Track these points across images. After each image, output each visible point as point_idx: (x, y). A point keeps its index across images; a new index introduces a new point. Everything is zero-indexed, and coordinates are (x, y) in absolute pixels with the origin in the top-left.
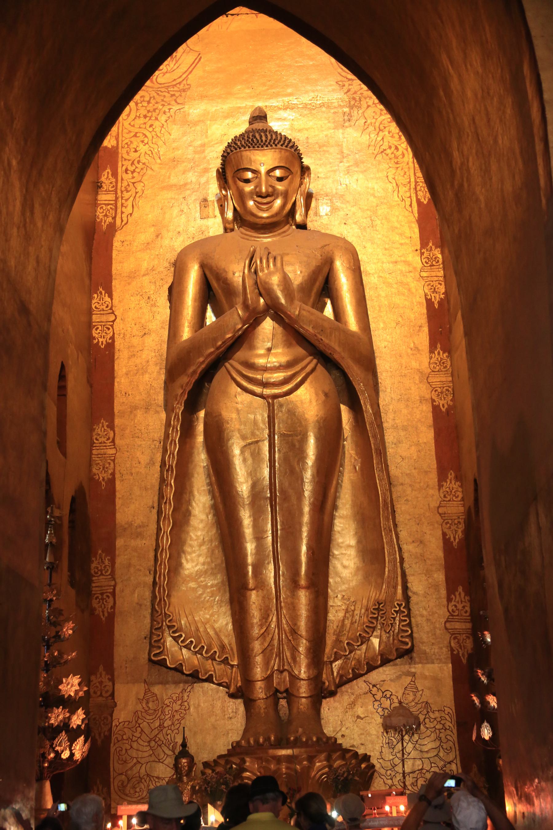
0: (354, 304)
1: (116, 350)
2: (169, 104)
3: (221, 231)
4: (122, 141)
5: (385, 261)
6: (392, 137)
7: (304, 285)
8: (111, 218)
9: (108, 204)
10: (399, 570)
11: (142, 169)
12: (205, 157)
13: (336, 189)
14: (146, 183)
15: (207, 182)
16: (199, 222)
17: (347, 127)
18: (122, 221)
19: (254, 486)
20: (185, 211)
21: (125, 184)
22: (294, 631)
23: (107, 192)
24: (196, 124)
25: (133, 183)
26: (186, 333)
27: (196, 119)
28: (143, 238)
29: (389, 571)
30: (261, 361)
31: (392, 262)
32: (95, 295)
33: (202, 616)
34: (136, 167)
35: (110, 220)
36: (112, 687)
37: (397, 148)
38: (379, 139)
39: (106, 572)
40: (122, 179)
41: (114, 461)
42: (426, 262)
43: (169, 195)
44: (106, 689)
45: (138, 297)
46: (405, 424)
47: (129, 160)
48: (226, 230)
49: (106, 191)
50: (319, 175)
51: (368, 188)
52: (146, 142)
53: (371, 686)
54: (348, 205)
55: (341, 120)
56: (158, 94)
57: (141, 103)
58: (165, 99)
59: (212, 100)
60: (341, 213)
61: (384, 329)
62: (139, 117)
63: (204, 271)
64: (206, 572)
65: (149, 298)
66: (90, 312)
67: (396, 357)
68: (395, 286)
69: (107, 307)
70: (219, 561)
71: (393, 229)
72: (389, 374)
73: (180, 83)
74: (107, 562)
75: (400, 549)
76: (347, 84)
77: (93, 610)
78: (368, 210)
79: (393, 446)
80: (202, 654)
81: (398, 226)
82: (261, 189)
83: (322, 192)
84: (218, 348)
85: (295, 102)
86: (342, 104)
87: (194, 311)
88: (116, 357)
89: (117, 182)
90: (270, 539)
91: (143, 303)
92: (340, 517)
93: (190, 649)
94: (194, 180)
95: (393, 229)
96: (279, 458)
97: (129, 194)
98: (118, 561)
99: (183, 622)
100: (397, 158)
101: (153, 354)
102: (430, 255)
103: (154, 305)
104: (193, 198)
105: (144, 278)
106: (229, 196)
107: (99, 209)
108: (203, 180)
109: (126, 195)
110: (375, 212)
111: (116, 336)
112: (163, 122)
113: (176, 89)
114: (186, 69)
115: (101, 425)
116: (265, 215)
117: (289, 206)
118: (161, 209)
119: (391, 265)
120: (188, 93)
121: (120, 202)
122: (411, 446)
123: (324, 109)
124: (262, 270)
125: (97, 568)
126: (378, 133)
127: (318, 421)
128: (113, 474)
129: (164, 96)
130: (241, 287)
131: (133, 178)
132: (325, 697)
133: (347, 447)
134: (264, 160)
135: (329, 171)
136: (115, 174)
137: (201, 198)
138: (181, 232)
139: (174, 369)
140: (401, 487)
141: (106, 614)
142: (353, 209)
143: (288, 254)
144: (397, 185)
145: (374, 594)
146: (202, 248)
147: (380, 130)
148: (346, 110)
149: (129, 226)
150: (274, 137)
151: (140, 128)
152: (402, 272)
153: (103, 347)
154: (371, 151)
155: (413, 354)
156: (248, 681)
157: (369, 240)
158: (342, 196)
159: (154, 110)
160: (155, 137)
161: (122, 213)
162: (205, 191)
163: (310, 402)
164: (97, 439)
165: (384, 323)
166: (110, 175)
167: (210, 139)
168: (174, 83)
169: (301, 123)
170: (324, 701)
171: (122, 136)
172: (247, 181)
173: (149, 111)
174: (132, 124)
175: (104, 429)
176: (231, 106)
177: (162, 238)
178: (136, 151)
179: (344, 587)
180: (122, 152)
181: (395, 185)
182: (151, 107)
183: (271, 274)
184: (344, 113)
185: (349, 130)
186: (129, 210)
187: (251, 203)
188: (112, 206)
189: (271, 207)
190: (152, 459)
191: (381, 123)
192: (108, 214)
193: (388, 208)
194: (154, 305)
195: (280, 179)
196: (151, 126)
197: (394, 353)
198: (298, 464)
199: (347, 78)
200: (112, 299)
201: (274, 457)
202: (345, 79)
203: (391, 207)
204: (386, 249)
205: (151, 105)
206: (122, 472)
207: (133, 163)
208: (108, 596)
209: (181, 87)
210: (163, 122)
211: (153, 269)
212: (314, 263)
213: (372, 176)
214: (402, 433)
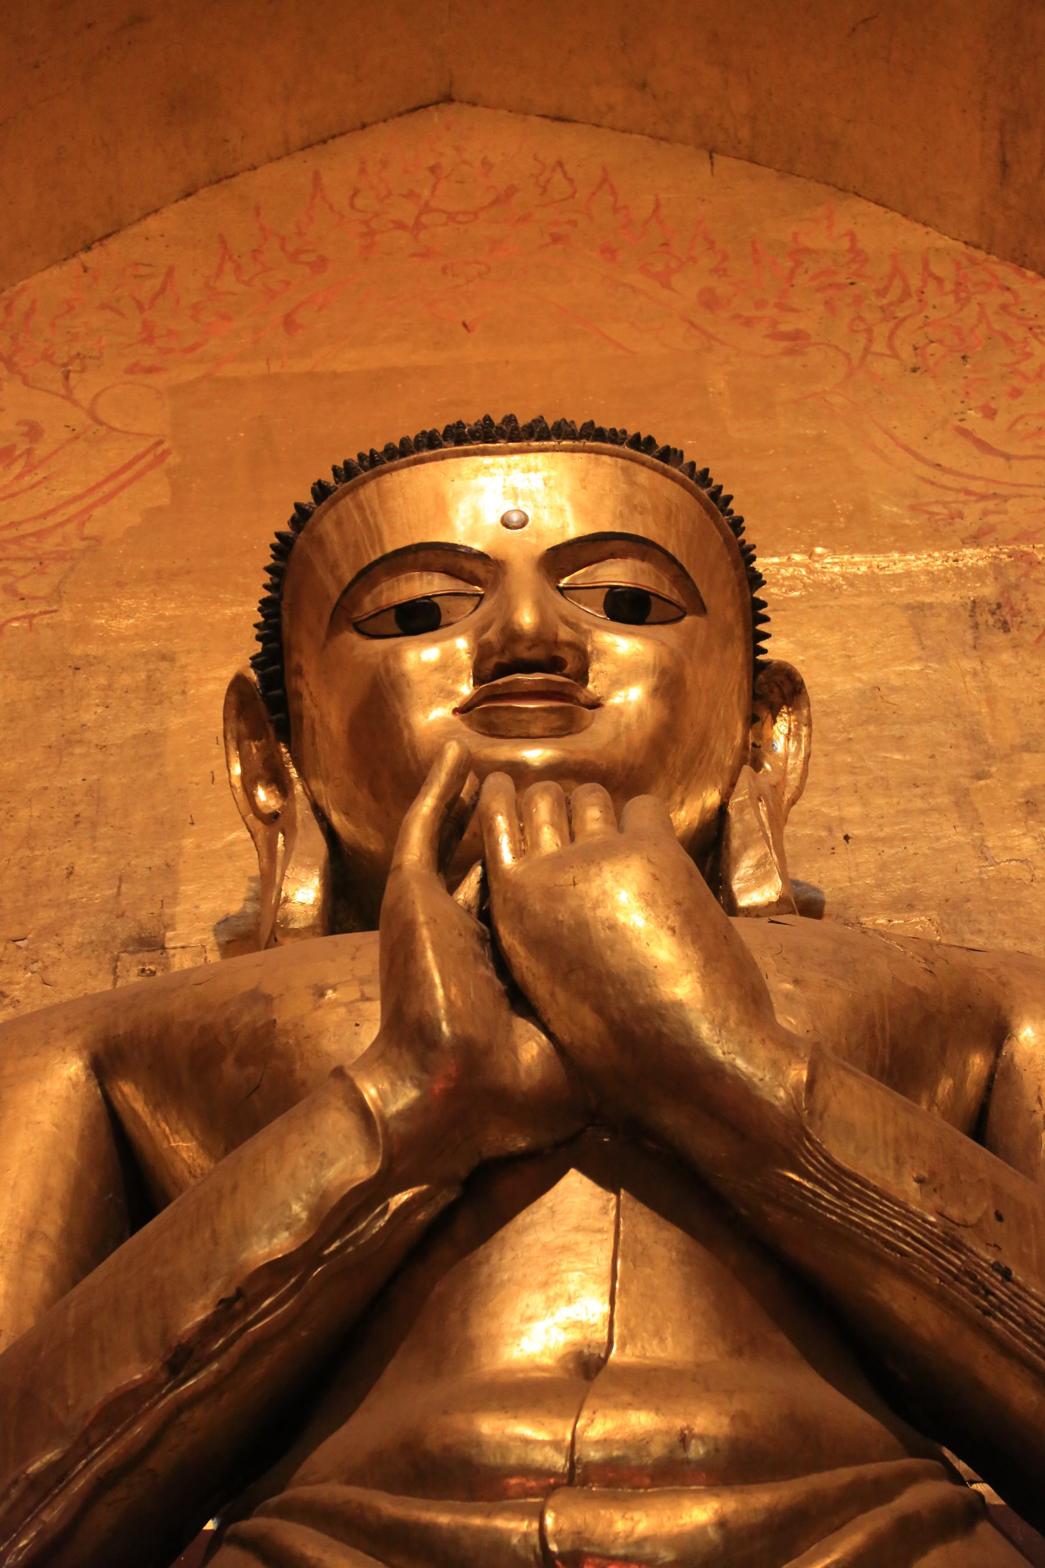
30: (529, 1435)
50: (854, 831)
63: (107, 1100)
73: (39, 535)
84: (181, 1360)
104: (75, 935)
114: (78, 490)
137: (124, 930)
172: (421, 619)
199: (968, 493)
202: (962, 497)
209: (49, 544)
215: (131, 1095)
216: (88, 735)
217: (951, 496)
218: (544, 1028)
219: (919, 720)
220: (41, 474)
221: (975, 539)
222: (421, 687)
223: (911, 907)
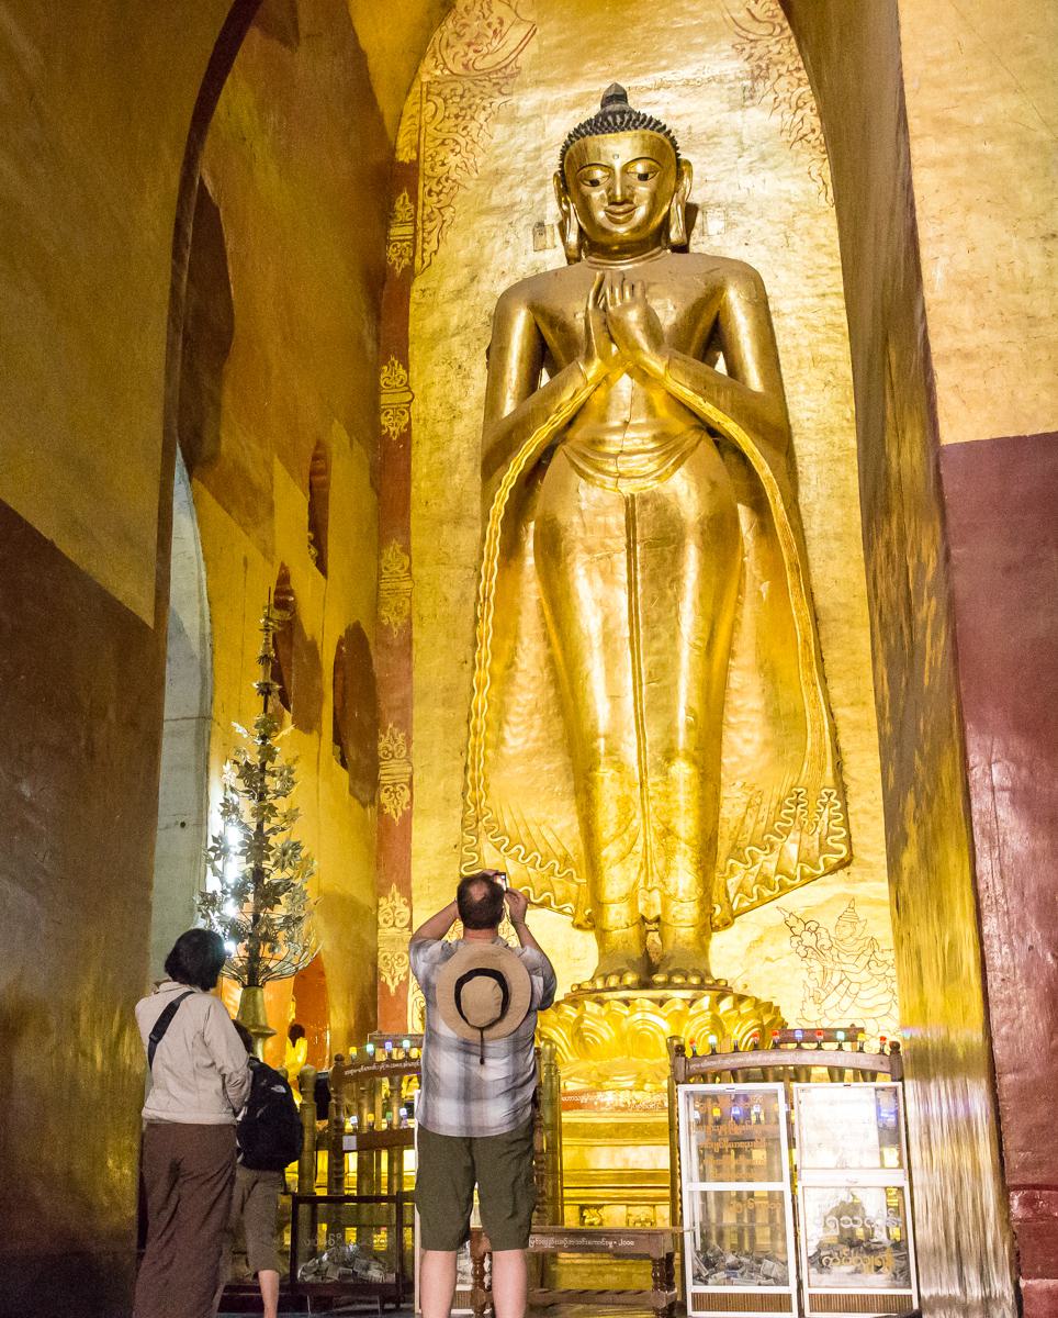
0: (756, 352)
1: (414, 442)
2: (490, 97)
3: (566, 264)
7: (679, 326)
8: (407, 260)
9: (404, 241)
10: (828, 743)
12: (540, 166)
13: (733, 196)
14: (457, 207)
15: (544, 200)
16: (532, 255)
17: (747, 107)
18: (423, 262)
19: (606, 620)
20: (512, 241)
21: (428, 210)
22: (668, 832)
23: (404, 223)
24: (528, 120)
25: (439, 209)
26: (509, 406)
27: (530, 113)
28: (451, 284)
29: (813, 744)
31: (817, 296)
32: (385, 368)
33: (533, 813)
34: (444, 187)
35: (406, 261)
36: (409, 915)
38: (797, 119)
39: (399, 755)
40: (424, 205)
41: (410, 598)
43: (488, 221)
44: (401, 917)
45: (444, 367)
46: (839, 530)
48: (570, 260)
49: (401, 222)
51: (780, 191)
52: (457, 150)
53: (787, 915)
56: (475, 85)
60: (741, 230)
61: (806, 392)
62: (448, 118)
64: (538, 752)
65: (460, 367)
66: (376, 391)
68: (822, 330)
69: (401, 382)
70: (560, 736)
71: (819, 247)
72: (814, 458)
73: (506, 67)
74: (400, 740)
75: (831, 715)
76: (747, 47)
77: (381, 807)
78: (780, 222)
79: (821, 563)
80: (534, 868)
81: (827, 243)
83: (712, 202)
85: (672, 78)
86: (741, 76)
87: (520, 375)
88: (413, 452)
89: (416, 208)
90: (630, 698)
91: (451, 376)
92: (738, 669)
93: (517, 860)
94: (525, 197)
95: (819, 247)
96: (643, 580)
97: (434, 223)
98: (416, 736)
99: (506, 823)
101: (466, 446)
103: (467, 377)
104: (524, 222)
105: (453, 339)
106: (572, 212)
109: (429, 226)
110: (791, 225)
112: (482, 121)
113: (500, 75)
115: (392, 548)
116: (622, 230)
117: (658, 220)
118: (478, 242)
119: (816, 300)
120: (518, 79)
122: (848, 563)
123: (714, 84)
124: (614, 303)
125: (387, 749)
127: (701, 522)
128: (409, 618)
130: (583, 334)
131: (439, 201)
132: (717, 929)
133: (748, 567)
134: (621, 149)
136: (414, 198)
137: (535, 221)
138: (506, 272)
139: (493, 459)
140: (833, 623)
141: (400, 814)
142: (759, 223)
143: (655, 284)
145: (791, 779)
146: (533, 291)
147: (798, 108)
148: (748, 83)
149: (432, 268)
150: (634, 117)
152: (832, 308)
153: (395, 439)
154: (784, 139)
156: (598, 904)
157: (784, 265)
158: (742, 205)
159: (470, 107)
160: (470, 142)
161: (424, 250)
162: (540, 213)
163: (689, 492)
164: (386, 568)
165: (806, 383)
166: (407, 200)
167: (547, 139)
168: (498, 67)
169: (680, 107)
170: (714, 934)
172: (595, 183)
173: (462, 109)
174: (438, 128)
175: (397, 554)
176: (577, 91)
177: (478, 282)
178: (443, 164)
179: (745, 770)
180: (425, 166)
183: (626, 307)
185: (752, 111)
187: (600, 215)
189: (630, 218)
190: (462, 595)
191: (799, 98)
193: (812, 218)
194: (467, 377)
195: (643, 177)
196: (465, 128)
198: (671, 587)
200: (408, 372)
201: (636, 578)
203: (815, 216)
204: (808, 277)
206: (421, 612)
207: (439, 182)
208: (402, 788)
209: (508, 71)
211: (466, 327)
212: (696, 295)
213: (787, 173)
214: (835, 545)
215: (540, 321)
220: (504, 40)
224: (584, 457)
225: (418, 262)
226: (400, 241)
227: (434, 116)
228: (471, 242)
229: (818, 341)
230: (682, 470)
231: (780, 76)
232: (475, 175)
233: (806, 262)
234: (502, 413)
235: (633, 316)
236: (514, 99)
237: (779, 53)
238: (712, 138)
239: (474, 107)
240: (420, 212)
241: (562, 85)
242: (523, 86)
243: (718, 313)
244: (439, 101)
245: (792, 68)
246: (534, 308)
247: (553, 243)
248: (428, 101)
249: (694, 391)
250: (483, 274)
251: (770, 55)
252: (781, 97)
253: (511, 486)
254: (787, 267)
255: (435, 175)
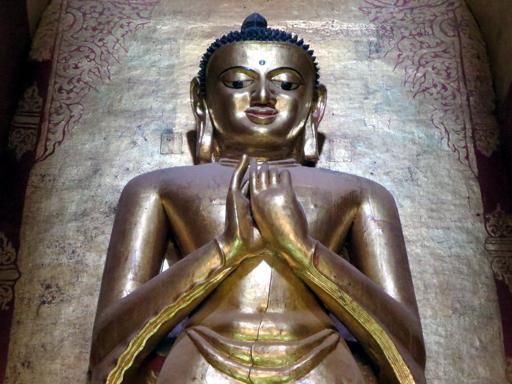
2: (129, 18)
3: (191, 164)
4: (59, 55)
5: (431, 225)
6: (438, 73)
11: (82, 89)
12: (173, 81)
16: (157, 157)
20: (139, 143)
23: (31, 114)
24: (163, 43)
25: (68, 105)
26: (128, 287)
31: (442, 228)
34: (75, 87)
35: (29, 147)
37: (444, 88)
38: (419, 75)
42: (493, 231)
47: (65, 77)
50: (335, 112)
54: (376, 150)
55: (366, 50)
57: (90, 14)
58: (124, 12)
59: (189, 17)
62: (86, 29)
65: (73, 252)
67: (453, 359)
68: (448, 259)
69: (9, 260)
78: (404, 159)
82: (259, 92)
83: (339, 133)
85: (303, 26)
89: (45, 102)
94: (155, 105)
97: (61, 117)
100: (446, 99)
102: (498, 223)
106: (208, 116)
107: (14, 133)
108: (169, 107)
111: (16, 300)
112: (119, 36)
116: (262, 130)
117: (294, 132)
119: (441, 231)
120: (156, 7)
121: (46, 126)
123: (341, 36)
126: (418, 68)
129: (124, 9)
135: (349, 108)
136: (43, 93)
137: (164, 127)
142: (386, 156)
144: (446, 131)
147: (420, 65)
151: (85, 41)
152: (457, 242)
155: (478, 357)
157: (408, 197)
159: (108, 23)
160: (105, 53)
161: (47, 139)
166: (36, 94)
167: (181, 60)
171: (60, 49)
172: (238, 85)
173: (100, 24)
174: (75, 36)
177: (101, 175)
178: (76, 67)
181: (443, 130)
182: (103, 19)
183: (272, 192)
184: (370, 43)
186: (59, 135)
187: (240, 114)
188: (33, 131)
191: (421, 57)
192: (26, 139)
195: (287, 87)
197: (449, 352)
199: (374, 5)
200: (17, 250)
202: (372, 6)
203: (438, 157)
204: (432, 210)
205: (103, 17)
210: (119, 36)
211: (84, 214)
216: (157, 64)
217: (369, 6)
218: (260, 232)
219: (353, 79)
221: (373, 21)
222: (238, 104)
223: (346, 138)
224: (214, 343)
225: (40, 151)
226: (24, 128)
227: (71, 26)
228: (97, 136)
229: (443, 270)
230: (321, 367)
231: (403, 37)
232: (107, 81)
233: (432, 197)
234: (121, 292)
235: (279, 201)
236: (152, 23)
237: (403, 20)
238: (342, 77)
239: (112, 24)
240: (48, 105)
241: (198, 18)
242: (162, 14)
243: (353, 223)
244: (79, 15)
245: (414, 32)
246: (167, 194)
247: (180, 150)
248: (67, 13)
249: (338, 285)
250: (106, 168)
251: (393, 20)
252: (405, 54)
253: (126, 369)
254: (411, 198)
255: (67, 75)
